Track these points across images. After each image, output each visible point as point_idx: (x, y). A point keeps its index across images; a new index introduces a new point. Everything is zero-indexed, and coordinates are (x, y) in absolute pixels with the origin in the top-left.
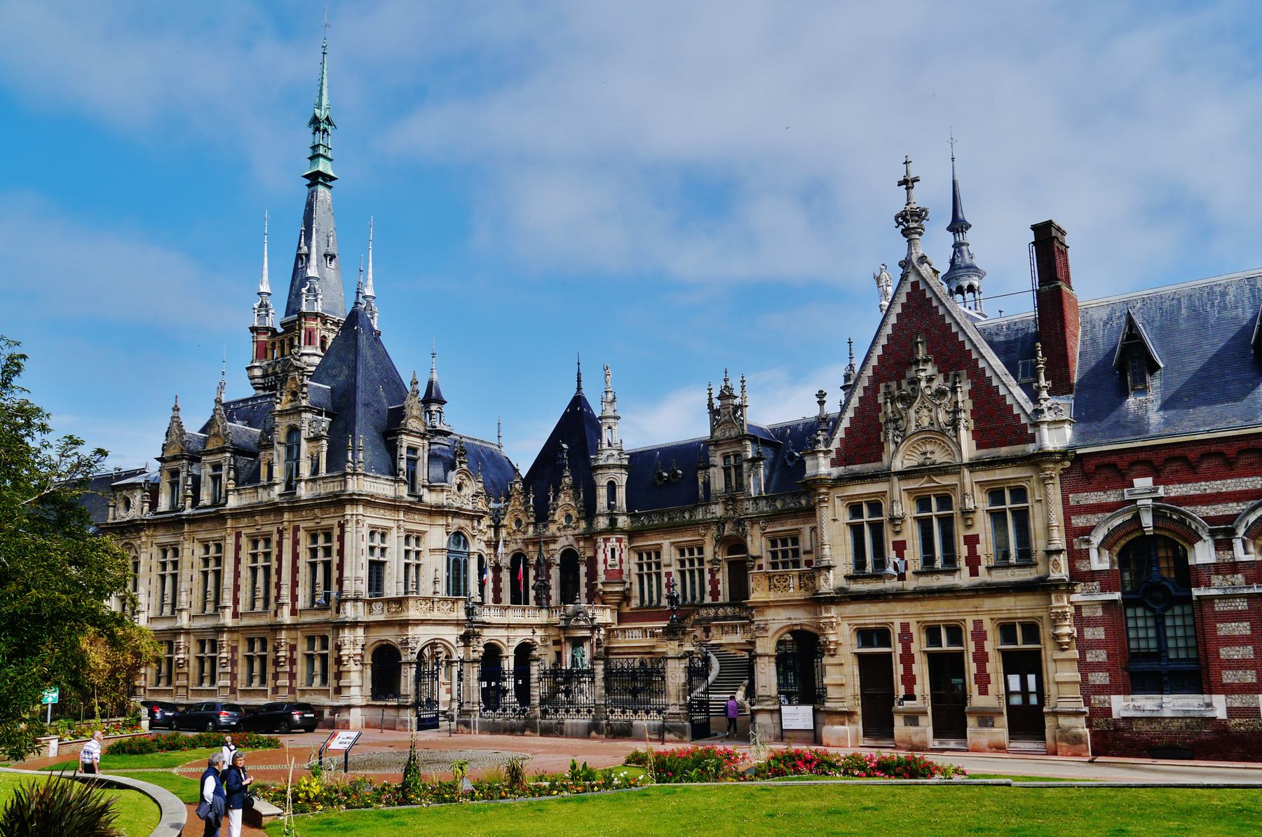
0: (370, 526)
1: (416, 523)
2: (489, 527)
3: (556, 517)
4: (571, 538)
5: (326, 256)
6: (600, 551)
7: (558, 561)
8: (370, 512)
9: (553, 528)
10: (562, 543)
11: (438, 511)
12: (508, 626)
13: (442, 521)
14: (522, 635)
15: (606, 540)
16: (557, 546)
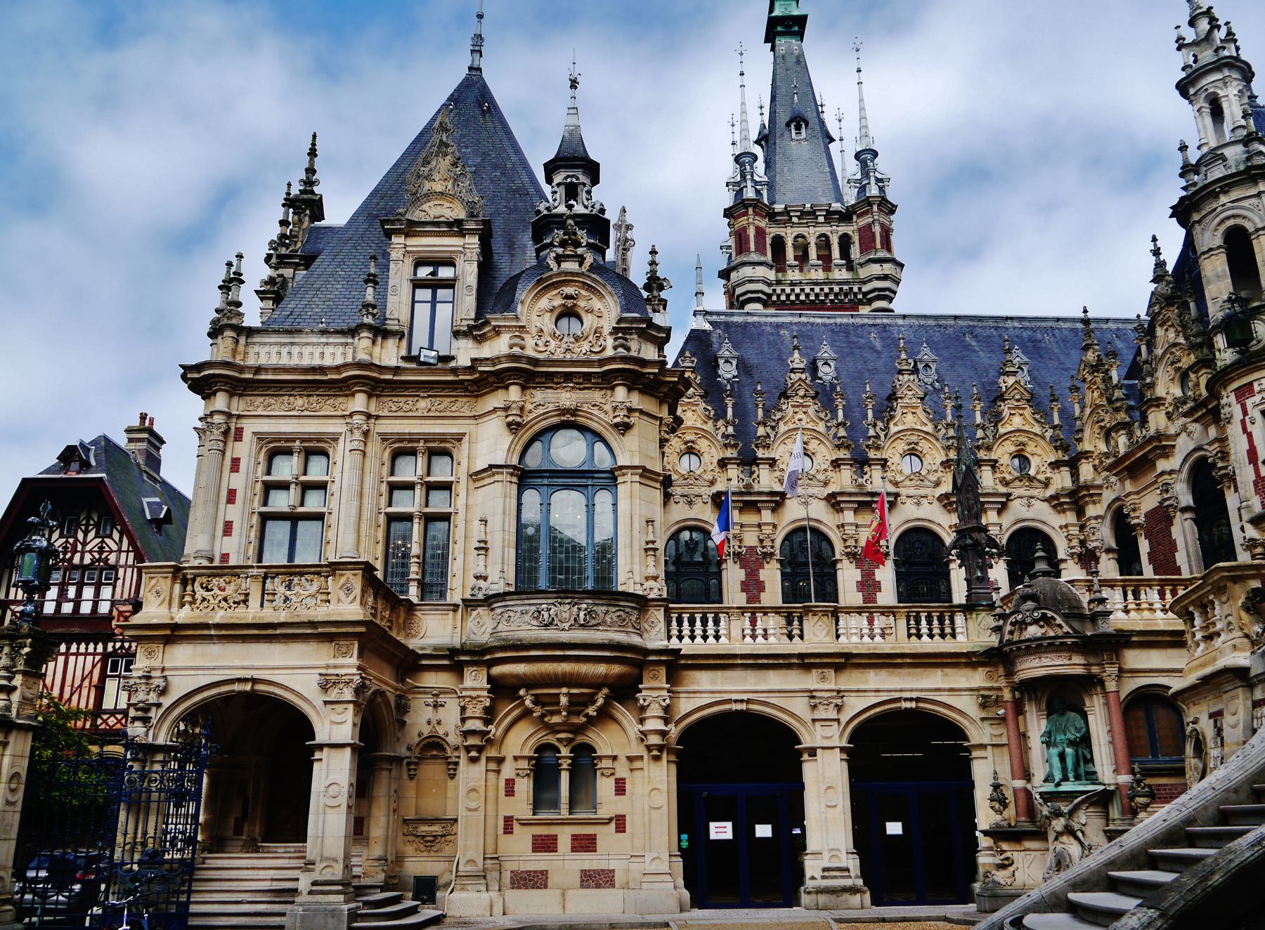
0: (261, 437)
1: (416, 418)
2: (1055, 465)
3: (1160, 391)
4: (1196, 428)
5: (788, 125)
6: (1234, 430)
7: (1186, 499)
8: (258, 404)
9: (1157, 420)
10: (1184, 445)
11: (480, 382)
12: (805, 662)
13: (496, 400)
14: (869, 691)
15: (1245, 392)
16: (1174, 462)
